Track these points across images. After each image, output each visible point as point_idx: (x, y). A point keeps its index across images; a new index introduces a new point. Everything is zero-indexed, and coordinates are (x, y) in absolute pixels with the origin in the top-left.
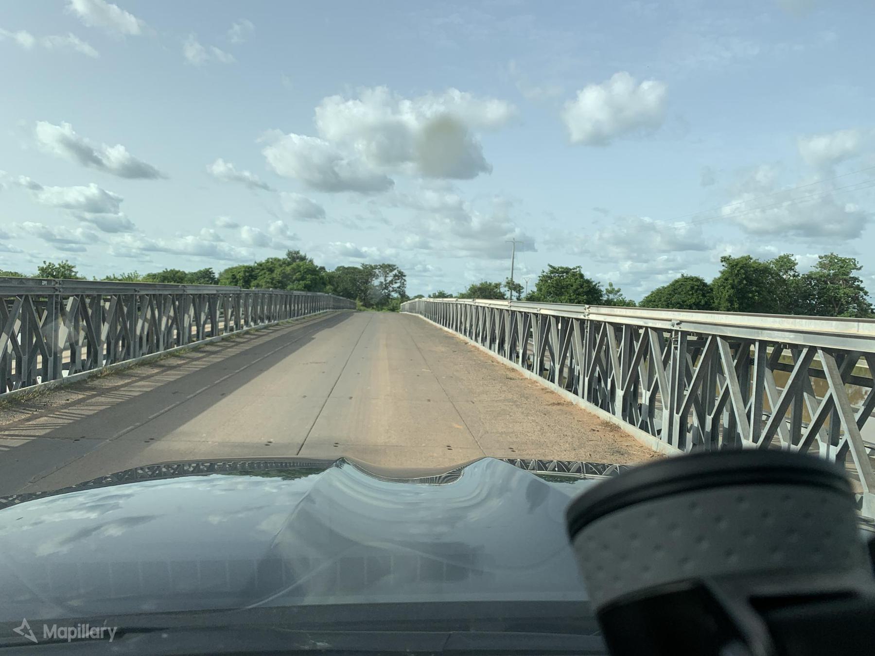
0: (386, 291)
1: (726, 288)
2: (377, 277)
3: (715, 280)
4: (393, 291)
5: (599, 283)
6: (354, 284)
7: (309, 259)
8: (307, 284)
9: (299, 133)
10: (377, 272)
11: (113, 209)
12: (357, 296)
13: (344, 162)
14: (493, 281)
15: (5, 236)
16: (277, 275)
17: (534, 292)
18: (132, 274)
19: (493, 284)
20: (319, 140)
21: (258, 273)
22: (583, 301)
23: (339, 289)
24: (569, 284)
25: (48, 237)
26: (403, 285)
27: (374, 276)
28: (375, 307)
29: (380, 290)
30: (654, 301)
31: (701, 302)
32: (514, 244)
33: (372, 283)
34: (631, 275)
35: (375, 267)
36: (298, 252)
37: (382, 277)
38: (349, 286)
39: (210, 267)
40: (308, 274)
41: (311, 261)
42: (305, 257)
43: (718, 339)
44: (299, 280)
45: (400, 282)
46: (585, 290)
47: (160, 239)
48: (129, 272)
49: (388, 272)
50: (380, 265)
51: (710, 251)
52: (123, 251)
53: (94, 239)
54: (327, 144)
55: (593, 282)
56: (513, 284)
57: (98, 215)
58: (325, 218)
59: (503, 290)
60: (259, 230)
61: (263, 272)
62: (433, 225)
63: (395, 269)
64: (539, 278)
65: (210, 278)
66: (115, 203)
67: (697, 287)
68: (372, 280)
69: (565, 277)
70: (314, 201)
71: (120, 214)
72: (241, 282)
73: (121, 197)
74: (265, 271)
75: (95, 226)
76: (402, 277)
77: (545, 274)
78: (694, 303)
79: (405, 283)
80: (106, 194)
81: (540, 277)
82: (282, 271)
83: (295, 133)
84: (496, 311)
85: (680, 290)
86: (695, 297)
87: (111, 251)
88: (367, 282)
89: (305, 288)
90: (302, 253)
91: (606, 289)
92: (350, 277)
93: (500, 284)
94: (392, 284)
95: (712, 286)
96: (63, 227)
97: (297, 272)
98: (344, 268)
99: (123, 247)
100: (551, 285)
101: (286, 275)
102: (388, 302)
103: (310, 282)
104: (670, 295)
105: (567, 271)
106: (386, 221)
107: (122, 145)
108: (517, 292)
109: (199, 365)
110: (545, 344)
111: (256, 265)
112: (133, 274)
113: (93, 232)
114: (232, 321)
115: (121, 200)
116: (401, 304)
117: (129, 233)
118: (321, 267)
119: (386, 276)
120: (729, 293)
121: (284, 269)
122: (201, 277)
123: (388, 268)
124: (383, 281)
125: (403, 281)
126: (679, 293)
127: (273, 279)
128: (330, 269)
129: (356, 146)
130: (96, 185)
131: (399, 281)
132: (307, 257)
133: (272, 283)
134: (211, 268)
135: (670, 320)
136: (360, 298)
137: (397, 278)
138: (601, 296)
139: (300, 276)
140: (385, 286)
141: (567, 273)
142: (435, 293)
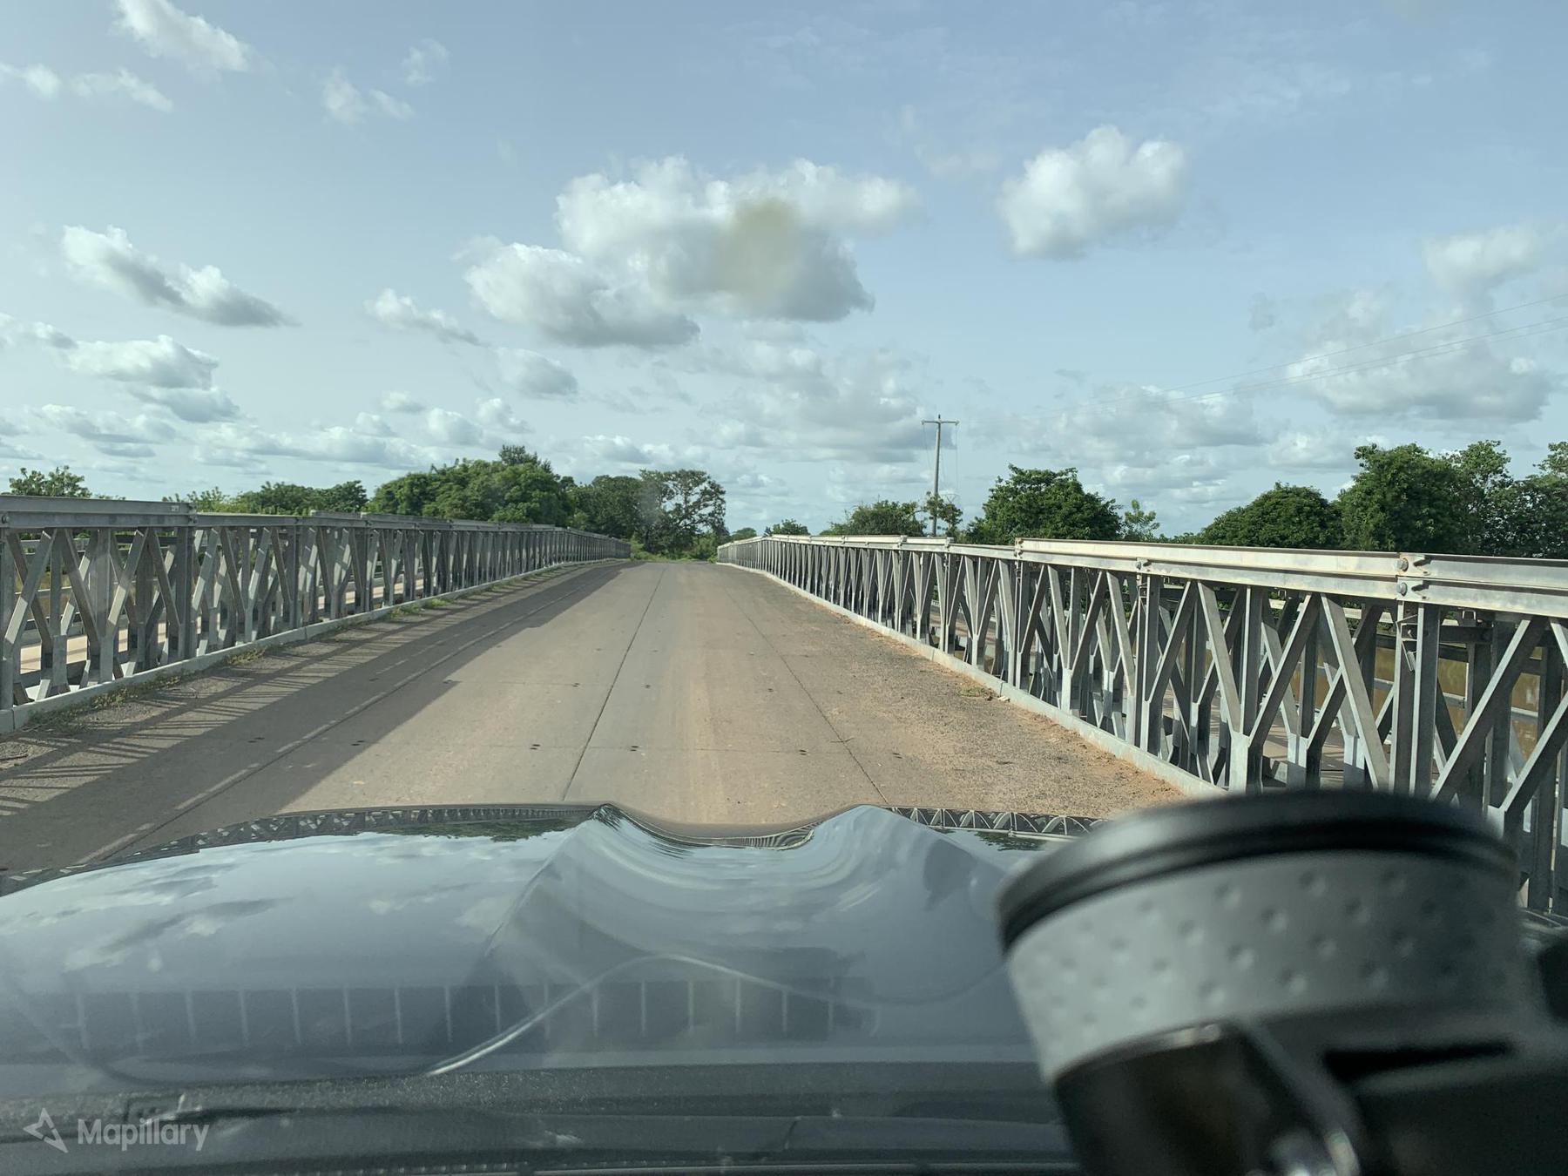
0: (688, 522)
1: (1369, 509)
2: (671, 495)
3: (1343, 495)
4: (700, 522)
5: (1113, 501)
7: (542, 463)
8: (533, 509)
9: (528, 242)
10: (671, 486)
11: (200, 381)
12: (632, 531)
13: (610, 293)
14: (900, 498)
15: (9, 431)
16: (472, 491)
17: (980, 521)
18: (208, 494)
19: (900, 505)
20: (564, 255)
21: (438, 488)
23: (599, 518)
24: (1053, 505)
25: (87, 431)
26: (720, 509)
27: (665, 493)
28: (667, 551)
29: (675, 520)
30: (1223, 537)
31: (1317, 537)
32: (939, 424)
33: (662, 507)
34: (1125, 490)
35: (667, 477)
36: (522, 450)
38: (617, 513)
39: (357, 479)
41: (546, 468)
42: (535, 458)
44: (516, 502)
45: (715, 504)
48: (204, 491)
49: (691, 485)
50: (675, 473)
52: (219, 454)
53: (167, 433)
54: (579, 261)
55: (1103, 499)
56: (941, 506)
57: (174, 391)
58: (575, 392)
59: (919, 516)
61: (446, 486)
62: (769, 402)
64: (991, 494)
65: (358, 500)
66: (205, 370)
68: (661, 501)
69: (1043, 490)
70: (557, 363)
71: (214, 390)
72: (403, 507)
73: (214, 359)
74: (451, 483)
75: (168, 410)
77: (1003, 484)
79: (723, 506)
81: (993, 491)
82: (482, 483)
83: (521, 243)
85: (1274, 515)
86: (1305, 528)
87: (197, 455)
89: (527, 516)
90: (529, 452)
91: (1126, 514)
92: (621, 496)
93: (914, 505)
94: (699, 509)
95: (1338, 507)
96: (112, 413)
97: (513, 486)
99: (220, 447)
100: (1017, 505)
101: (490, 490)
103: (538, 505)
104: (1254, 523)
105: (1048, 478)
106: (685, 397)
108: (948, 521)
109: (320, 671)
111: (434, 472)
112: (211, 493)
113: (165, 421)
114: (401, 582)
115: (215, 365)
116: (719, 547)
117: (230, 424)
119: (687, 494)
120: (1375, 520)
121: (487, 480)
122: (339, 499)
123: (690, 478)
124: (682, 502)
126: (1273, 521)
127: (465, 499)
129: (630, 263)
130: (171, 339)
132: (538, 459)
133: (463, 507)
134: (359, 482)
136: (640, 535)
138: (1118, 527)
139: (519, 493)
140: (687, 511)
141: (1048, 482)
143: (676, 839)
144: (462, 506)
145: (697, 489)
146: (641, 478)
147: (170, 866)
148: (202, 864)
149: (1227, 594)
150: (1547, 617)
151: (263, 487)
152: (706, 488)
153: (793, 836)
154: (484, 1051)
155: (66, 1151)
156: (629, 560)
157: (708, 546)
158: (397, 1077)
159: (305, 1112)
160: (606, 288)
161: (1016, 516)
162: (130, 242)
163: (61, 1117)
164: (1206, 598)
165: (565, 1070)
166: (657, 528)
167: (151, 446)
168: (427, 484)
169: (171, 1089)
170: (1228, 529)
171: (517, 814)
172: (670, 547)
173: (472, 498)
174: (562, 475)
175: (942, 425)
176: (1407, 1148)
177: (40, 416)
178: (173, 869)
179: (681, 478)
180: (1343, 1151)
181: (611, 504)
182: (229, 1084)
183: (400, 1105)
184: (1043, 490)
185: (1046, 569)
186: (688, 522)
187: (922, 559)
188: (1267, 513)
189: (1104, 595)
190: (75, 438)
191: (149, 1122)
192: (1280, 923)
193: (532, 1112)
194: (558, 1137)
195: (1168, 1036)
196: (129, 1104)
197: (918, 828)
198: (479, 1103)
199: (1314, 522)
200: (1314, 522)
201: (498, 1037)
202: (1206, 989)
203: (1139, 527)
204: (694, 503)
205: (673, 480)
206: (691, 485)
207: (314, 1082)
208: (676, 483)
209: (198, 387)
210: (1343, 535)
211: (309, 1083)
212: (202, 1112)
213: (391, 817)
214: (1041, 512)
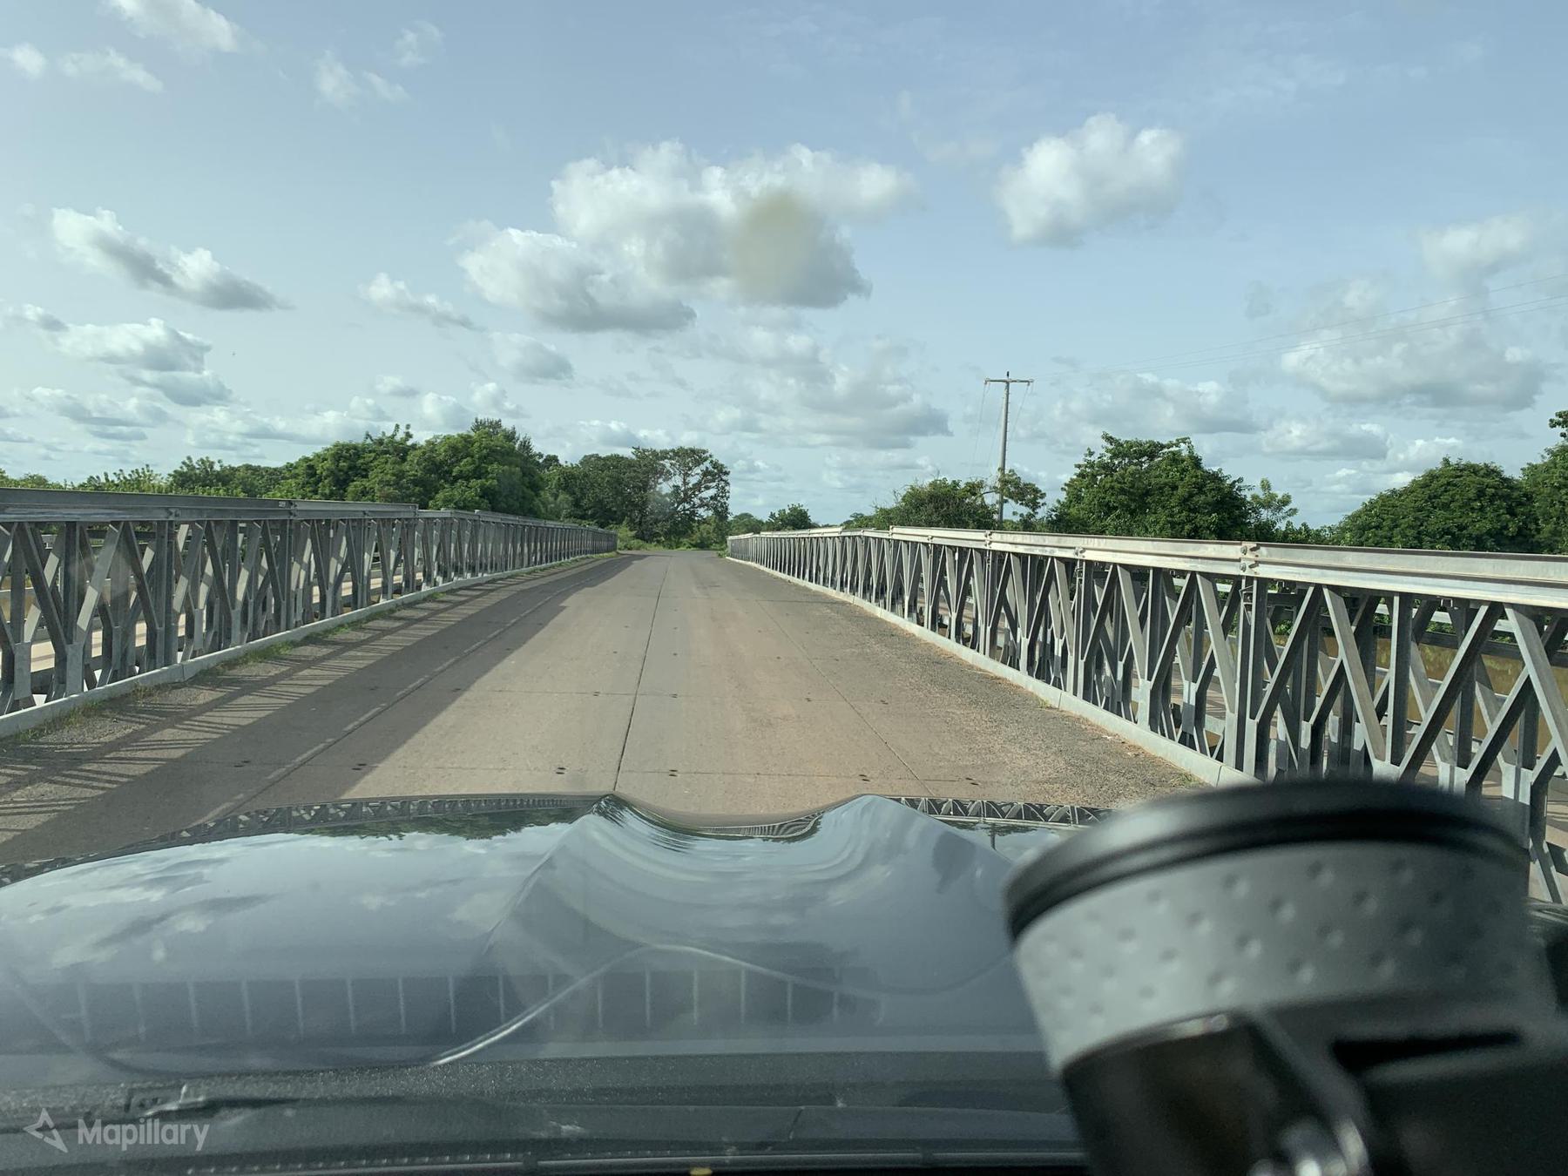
0: (687, 506)
2: (668, 476)
4: (700, 506)
5: (1240, 480)
7: (521, 439)
10: (668, 465)
12: (624, 515)
14: (959, 474)
16: (412, 467)
18: (137, 473)
19: (962, 485)
20: (559, 239)
22: (1208, 528)
23: (585, 501)
24: (1166, 484)
25: (78, 414)
26: (723, 492)
27: (661, 473)
30: (1377, 527)
31: (1506, 528)
32: (1008, 383)
33: (657, 489)
35: (664, 455)
37: (677, 476)
38: (607, 495)
41: (526, 446)
42: (514, 433)
43: (1326, 591)
44: (467, 479)
45: (717, 486)
46: (1209, 499)
47: (278, 418)
49: (690, 465)
50: (673, 451)
51: (1262, 433)
52: (212, 438)
53: (159, 417)
54: (574, 245)
55: (1228, 477)
58: (572, 377)
59: (991, 499)
60: (454, 399)
64: (1078, 471)
66: (197, 353)
67: (1493, 490)
70: (553, 348)
71: (206, 373)
72: (326, 487)
73: (207, 342)
75: (160, 393)
77: (1094, 458)
78: (1489, 533)
79: (727, 488)
80: (178, 337)
81: (1079, 466)
83: (513, 227)
84: (904, 546)
88: (645, 487)
93: (980, 485)
94: (700, 491)
96: (104, 397)
97: (462, 458)
98: (598, 458)
99: (213, 431)
100: (1117, 486)
102: (691, 528)
103: (495, 482)
105: (1152, 450)
106: (681, 383)
107: (206, 249)
108: (1027, 505)
110: (1000, 604)
111: (369, 441)
112: (140, 471)
113: (158, 405)
115: (208, 349)
116: (730, 538)
118: (549, 456)
119: (686, 475)
123: (690, 457)
124: (680, 484)
125: (722, 484)
126: (1446, 507)
127: (400, 475)
128: (569, 456)
129: (626, 249)
130: (162, 322)
131: (714, 484)
132: (517, 435)
133: (397, 484)
136: (632, 521)
139: (472, 467)
140: (685, 494)
142: (784, 510)
143: (679, 830)
145: (698, 470)
146: (634, 457)
147: (163, 860)
150: (1501, 603)
151: (184, 463)
153: (800, 828)
155: (66, 1151)
156: (613, 554)
158: (400, 1067)
159: (309, 1102)
160: (600, 273)
162: (120, 224)
163: (63, 1108)
165: (569, 1061)
167: (145, 430)
168: (359, 457)
169: (174, 1080)
171: (518, 803)
173: (411, 473)
175: (1011, 384)
176: (1416, 1140)
177: (31, 399)
180: (1353, 1144)
182: (230, 1075)
184: (1145, 466)
187: (957, 554)
191: (150, 1113)
192: (1288, 913)
194: (563, 1127)
197: (922, 821)
199: (1499, 507)
200: (1499, 507)
201: (502, 1027)
203: (1270, 514)
205: (670, 459)
206: (690, 465)
207: (317, 1072)
209: (190, 370)
210: (1537, 524)
211: (311, 1073)
212: (204, 1102)
213: (389, 808)
214: (1147, 493)
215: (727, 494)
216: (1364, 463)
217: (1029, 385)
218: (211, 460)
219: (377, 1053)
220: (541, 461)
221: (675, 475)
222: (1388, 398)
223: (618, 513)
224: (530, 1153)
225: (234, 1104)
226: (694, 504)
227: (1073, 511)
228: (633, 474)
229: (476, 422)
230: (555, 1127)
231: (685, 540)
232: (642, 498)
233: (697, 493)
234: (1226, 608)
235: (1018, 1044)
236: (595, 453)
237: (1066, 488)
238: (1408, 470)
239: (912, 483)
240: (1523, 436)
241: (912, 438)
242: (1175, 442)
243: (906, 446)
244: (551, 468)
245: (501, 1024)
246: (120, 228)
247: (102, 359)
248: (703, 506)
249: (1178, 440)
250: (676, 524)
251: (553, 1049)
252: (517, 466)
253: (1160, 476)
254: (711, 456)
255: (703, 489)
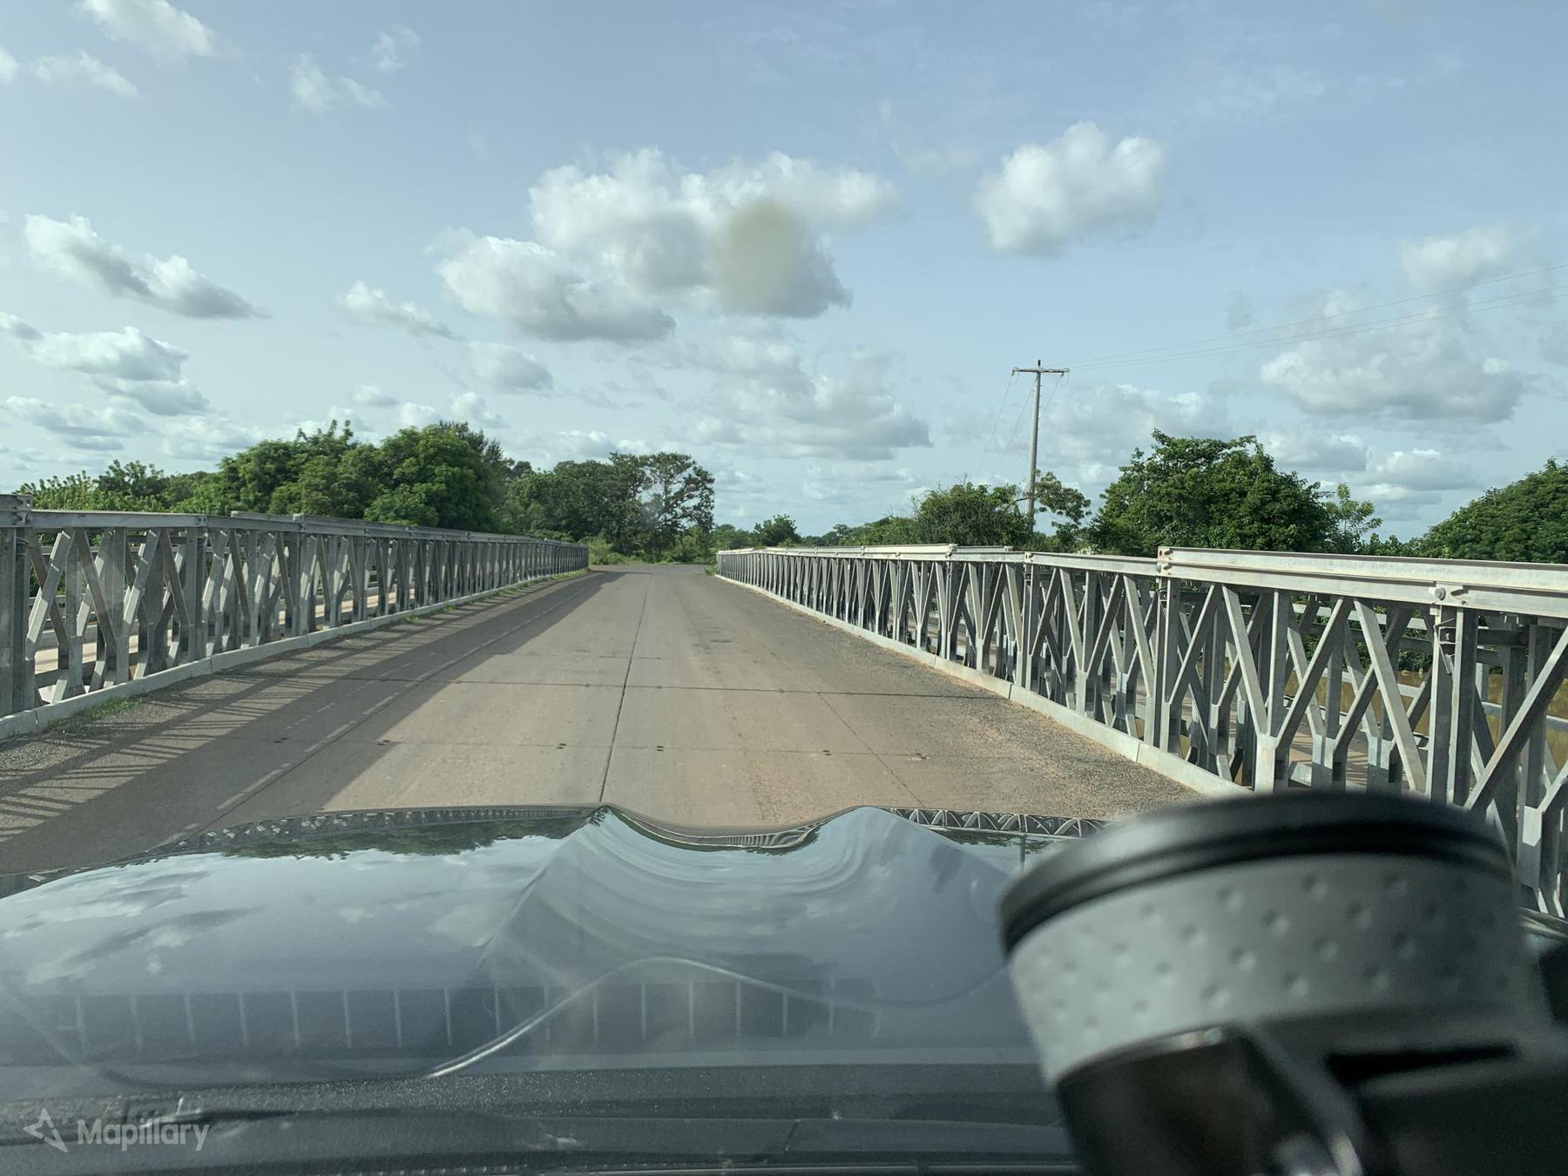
0: (669, 517)
2: (648, 484)
4: (683, 516)
5: (1316, 485)
6: (594, 502)
7: (490, 444)
8: (436, 493)
10: (648, 472)
11: (168, 373)
14: (987, 478)
19: (990, 491)
22: (1285, 542)
25: (53, 424)
26: (707, 501)
28: (642, 551)
29: (653, 515)
32: (1039, 373)
33: (637, 499)
35: (644, 461)
38: (582, 504)
40: (439, 464)
41: (494, 451)
48: (69, 476)
49: (672, 471)
50: (653, 457)
52: (189, 448)
53: (136, 426)
57: (140, 383)
63: (689, 466)
66: (174, 361)
71: (182, 382)
73: (184, 351)
75: (136, 402)
76: (703, 484)
77: (1144, 460)
79: (711, 497)
80: (154, 343)
87: (166, 449)
88: (624, 495)
92: (586, 484)
93: (1012, 491)
99: (190, 441)
102: (673, 540)
104: (1525, 520)
107: (181, 256)
113: (134, 414)
115: (184, 357)
118: (520, 462)
119: (668, 483)
123: (671, 463)
124: (661, 492)
128: (543, 464)
130: (137, 331)
131: (698, 493)
132: (485, 439)
135: (1434, 584)
136: (609, 532)
137: (692, 485)
142: (770, 521)
144: (328, 488)
145: (680, 477)
146: (611, 463)
148: (172, 872)
149: (1253, 598)
152: (690, 475)
154: (483, 1054)
157: (691, 545)
161: (1164, 506)
164: (1230, 601)
166: (631, 523)
167: (120, 440)
170: (1485, 528)
172: (648, 547)
174: (518, 459)
178: (143, 878)
179: (660, 462)
181: (574, 493)
183: (399, 1106)
185: (1058, 572)
186: (669, 517)
188: (1542, 505)
189: (1119, 599)
190: (42, 431)
193: (532, 1114)
195: (1174, 1039)
196: (128, 1105)
198: (479, 1106)
202: (1209, 991)
203: (1348, 525)
204: (675, 494)
205: (651, 465)
206: (672, 471)
208: (654, 469)
209: (167, 379)
215: (712, 504)
216: (1343, 475)
217: (1062, 375)
218: (142, 464)
219: (373, 1065)
220: (512, 468)
221: (655, 483)
222: (1366, 409)
223: (594, 524)
224: (526, 1166)
225: (231, 1116)
226: (676, 514)
227: (1120, 522)
228: (610, 482)
229: (441, 425)
230: (551, 1140)
231: (666, 553)
232: (620, 507)
233: (679, 502)
234: (1251, 622)
235: (1013, 1057)
236: (570, 459)
237: (1107, 495)
238: (1387, 482)
239: (935, 489)
240: (1501, 448)
241: (893, 449)
242: (1238, 441)
243: (888, 456)
244: (523, 475)
245: (495, 1037)
246: (95, 234)
247: (75, 368)
248: (686, 517)
249: (1241, 439)
250: (656, 535)
251: (551, 1061)
252: (470, 468)
253: (1224, 480)
254: (694, 463)
255: (685, 498)
